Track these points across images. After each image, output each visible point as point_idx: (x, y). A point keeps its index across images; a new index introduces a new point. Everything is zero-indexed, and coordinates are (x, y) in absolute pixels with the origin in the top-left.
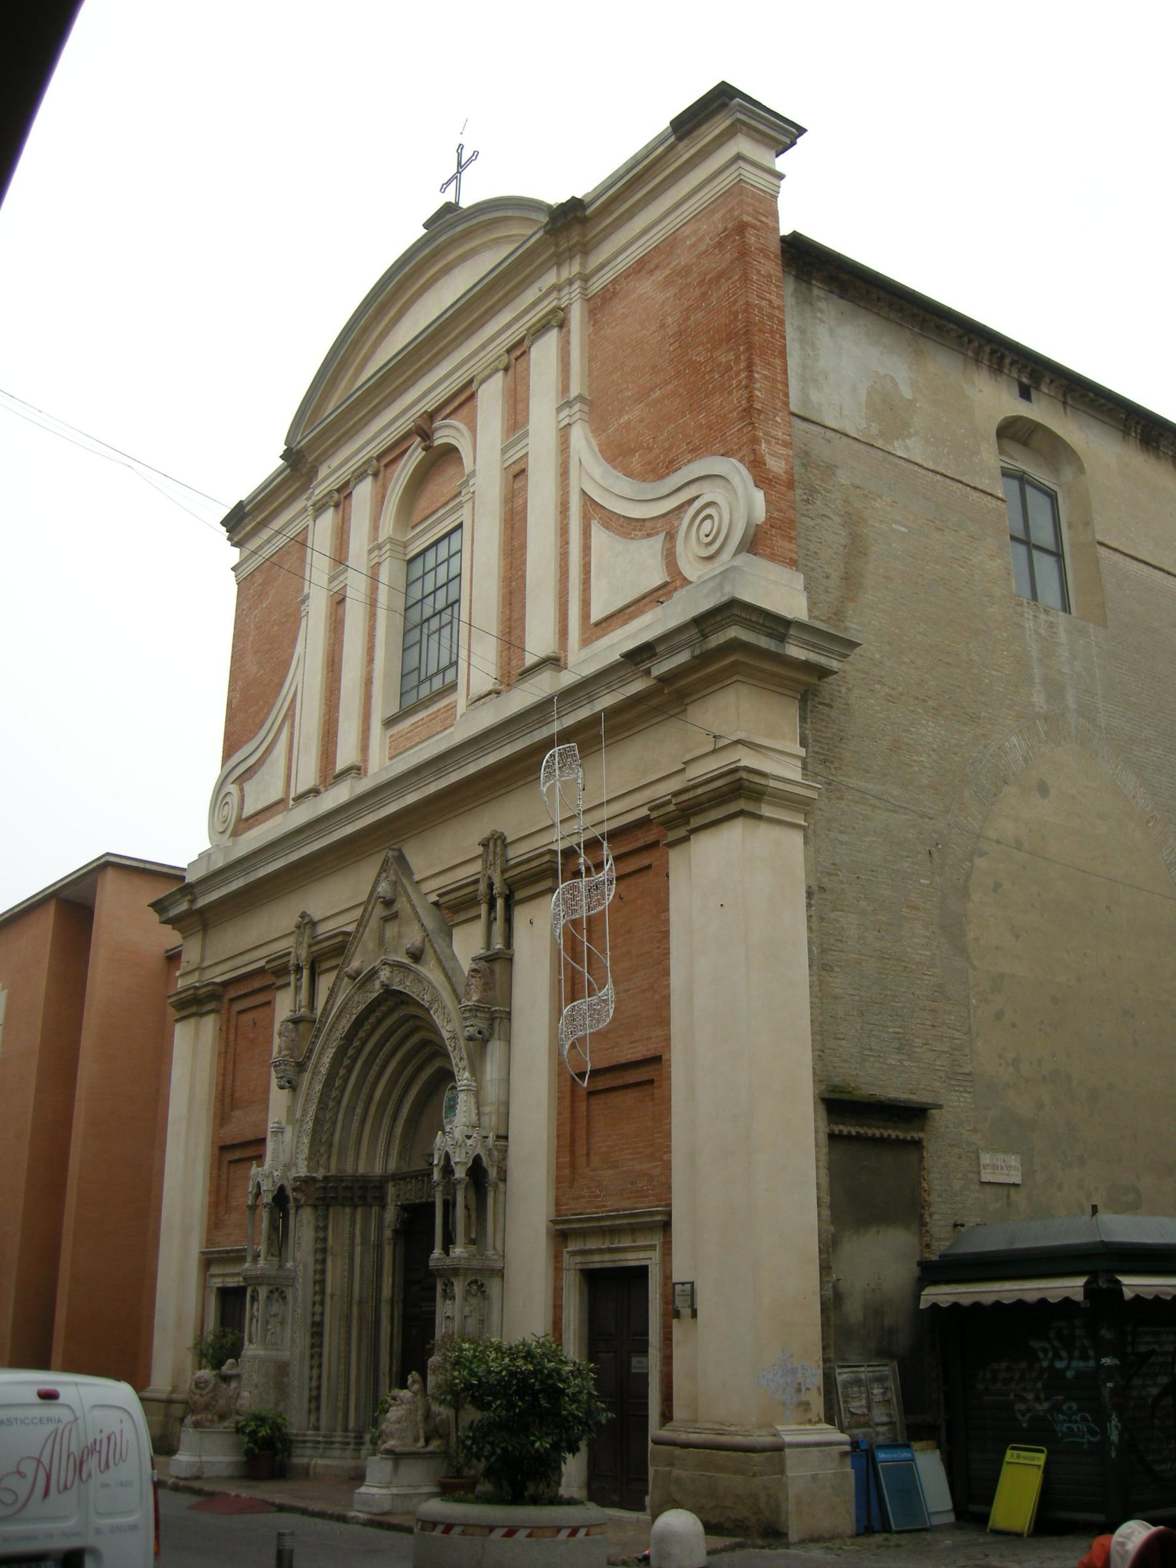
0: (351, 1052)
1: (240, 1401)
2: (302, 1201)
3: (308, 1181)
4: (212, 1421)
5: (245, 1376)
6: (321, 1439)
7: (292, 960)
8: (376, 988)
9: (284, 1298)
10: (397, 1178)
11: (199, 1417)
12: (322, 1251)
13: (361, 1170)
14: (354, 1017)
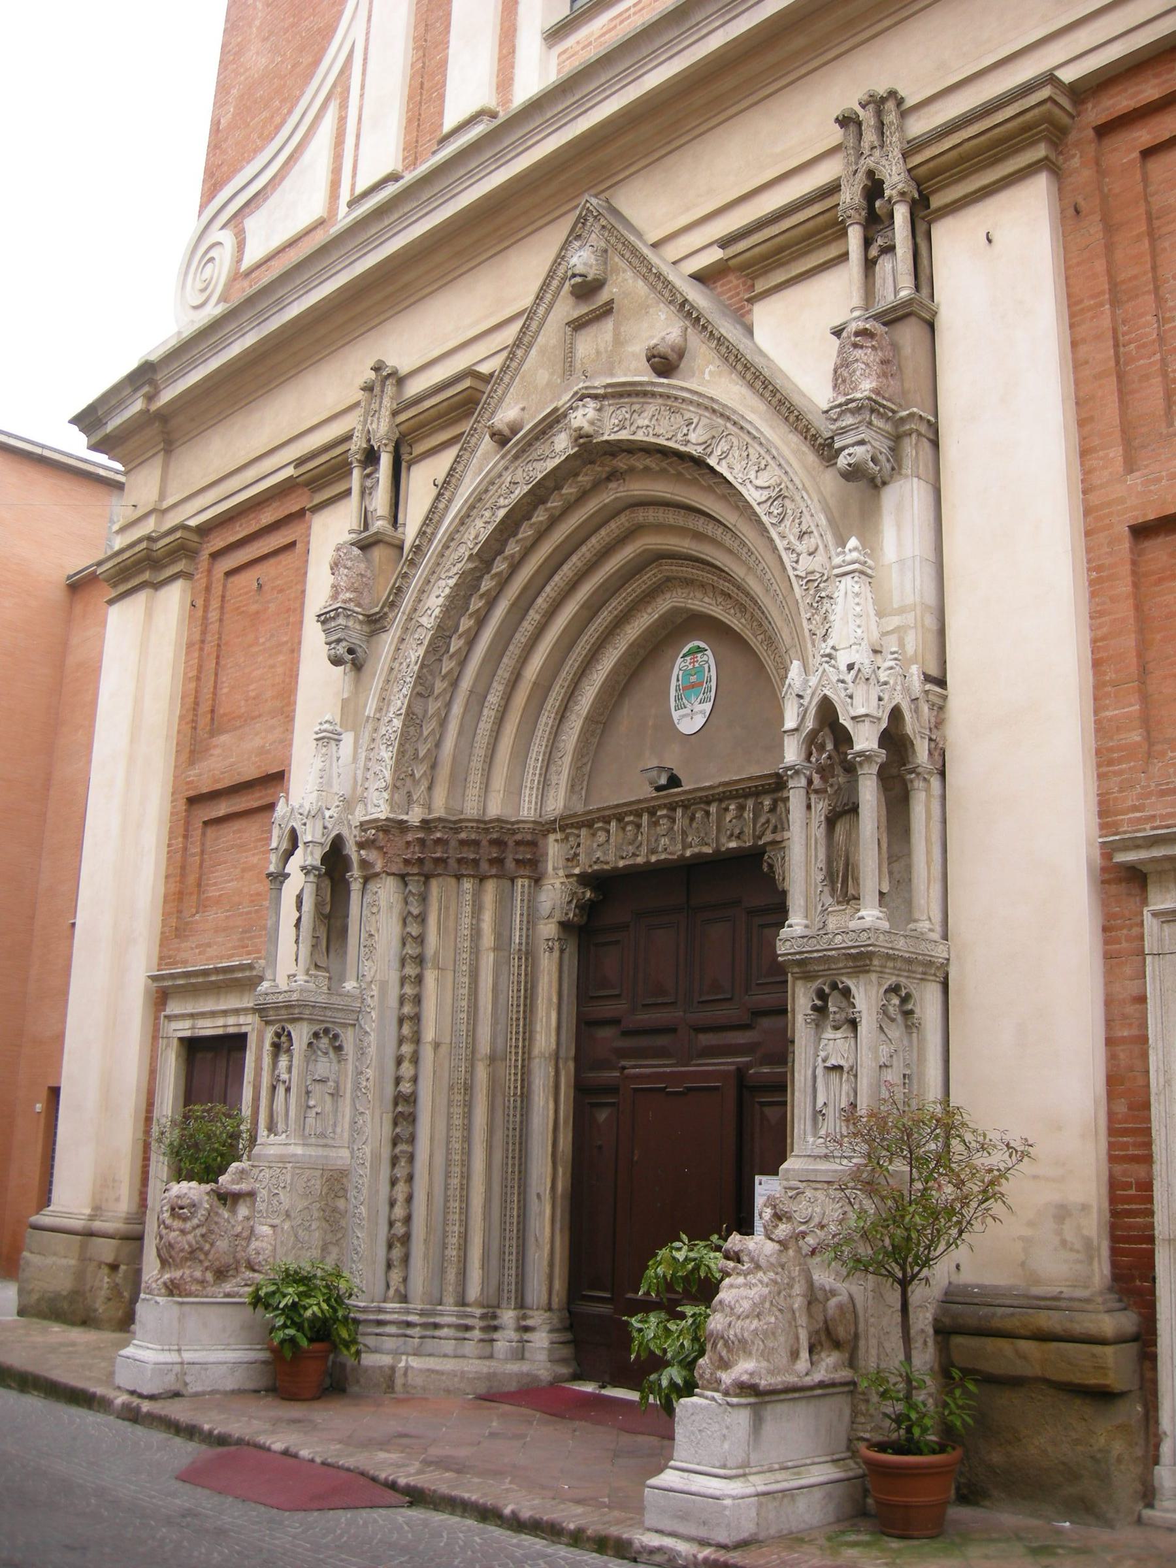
0: (487, 584)
1: (254, 1244)
2: (378, 868)
3: (392, 827)
4: (202, 1282)
5: (263, 1194)
6: (411, 1318)
7: (357, 445)
8: (562, 444)
9: (339, 1049)
10: (566, 825)
11: (177, 1274)
12: (414, 959)
13: (494, 810)
14: (501, 513)
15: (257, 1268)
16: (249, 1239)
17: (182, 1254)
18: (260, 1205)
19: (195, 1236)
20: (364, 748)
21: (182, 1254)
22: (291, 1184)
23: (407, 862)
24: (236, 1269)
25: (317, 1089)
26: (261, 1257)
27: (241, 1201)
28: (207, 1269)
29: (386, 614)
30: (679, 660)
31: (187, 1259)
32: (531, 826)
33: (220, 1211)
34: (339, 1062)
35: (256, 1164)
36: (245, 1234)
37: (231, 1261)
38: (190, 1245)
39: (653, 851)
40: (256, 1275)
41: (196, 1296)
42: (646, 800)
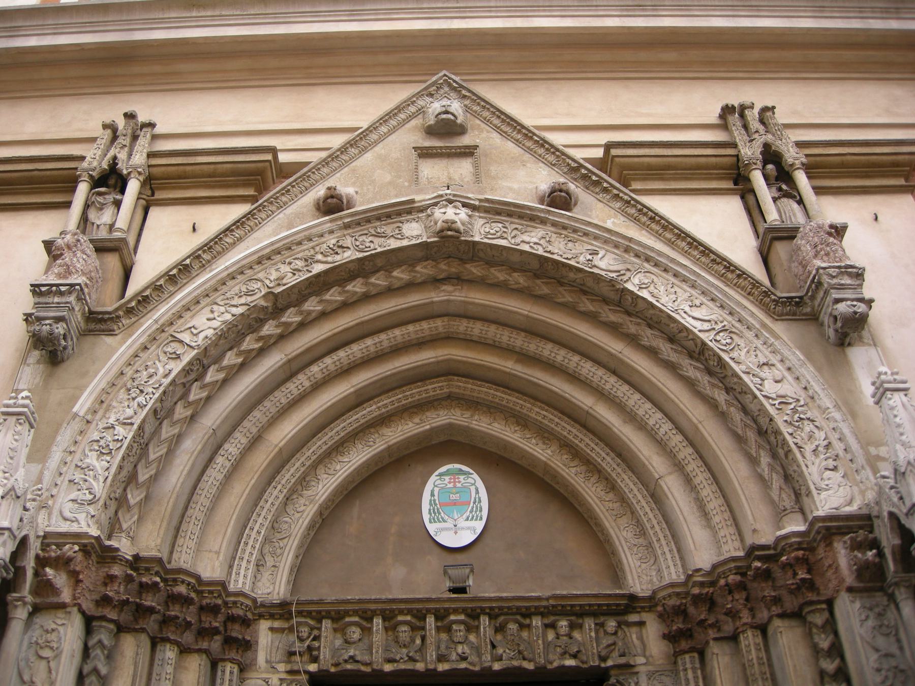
0: (269, 329)
3: (99, 552)
10: (280, 611)
13: (210, 568)
20: (61, 448)
23: (105, 600)
29: (118, 317)
30: (433, 478)
32: (249, 603)
39: (441, 658)
42: (438, 600)
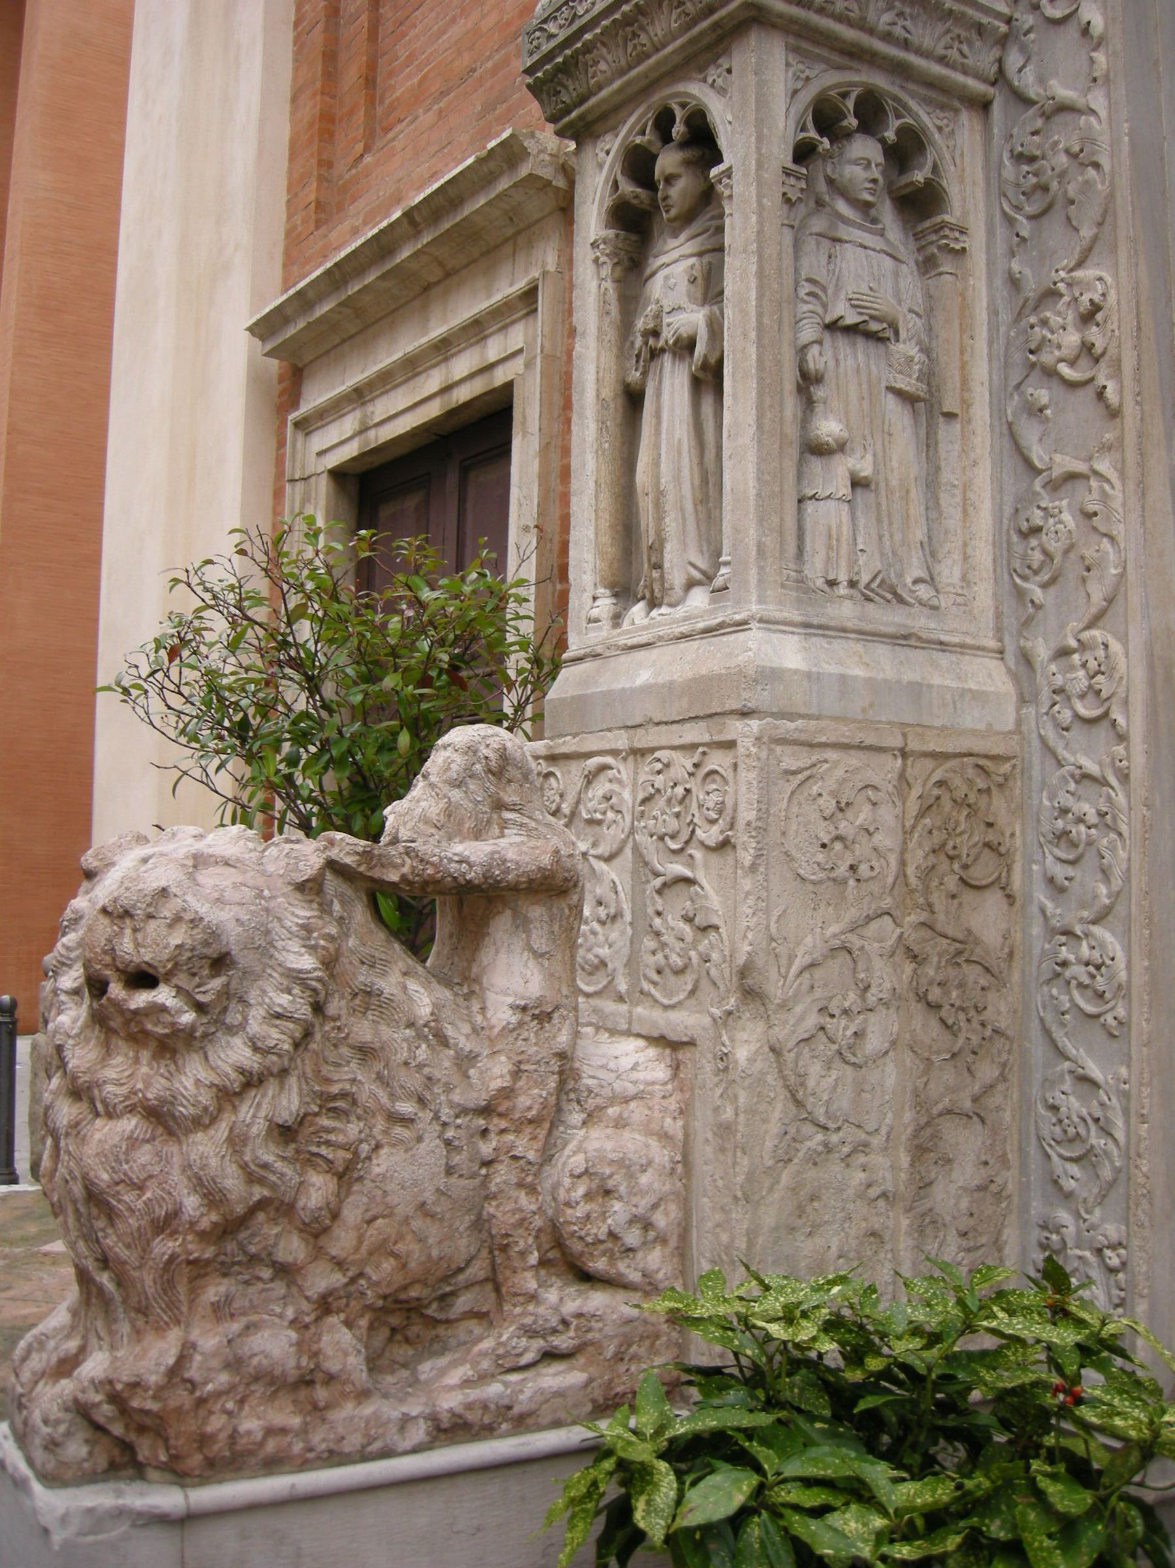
1: (586, 1145)
4: (306, 1383)
5: (608, 882)
9: (919, 204)
15: (599, 1265)
16: (550, 1120)
17: (164, 1247)
18: (603, 942)
19: (237, 1142)
21: (164, 1247)
22: (760, 829)
24: (494, 1281)
25: (845, 363)
26: (619, 1211)
27: (501, 925)
28: (325, 1305)
31: (199, 1269)
33: (389, 984)
34: (927, 265)
35: (568, 745)
36: (529, 1100)
37: (464, 1245)
38: (213, 1197)
40: (597, 1300)
41: (272, 1465)
